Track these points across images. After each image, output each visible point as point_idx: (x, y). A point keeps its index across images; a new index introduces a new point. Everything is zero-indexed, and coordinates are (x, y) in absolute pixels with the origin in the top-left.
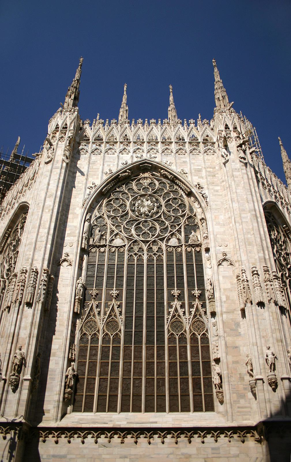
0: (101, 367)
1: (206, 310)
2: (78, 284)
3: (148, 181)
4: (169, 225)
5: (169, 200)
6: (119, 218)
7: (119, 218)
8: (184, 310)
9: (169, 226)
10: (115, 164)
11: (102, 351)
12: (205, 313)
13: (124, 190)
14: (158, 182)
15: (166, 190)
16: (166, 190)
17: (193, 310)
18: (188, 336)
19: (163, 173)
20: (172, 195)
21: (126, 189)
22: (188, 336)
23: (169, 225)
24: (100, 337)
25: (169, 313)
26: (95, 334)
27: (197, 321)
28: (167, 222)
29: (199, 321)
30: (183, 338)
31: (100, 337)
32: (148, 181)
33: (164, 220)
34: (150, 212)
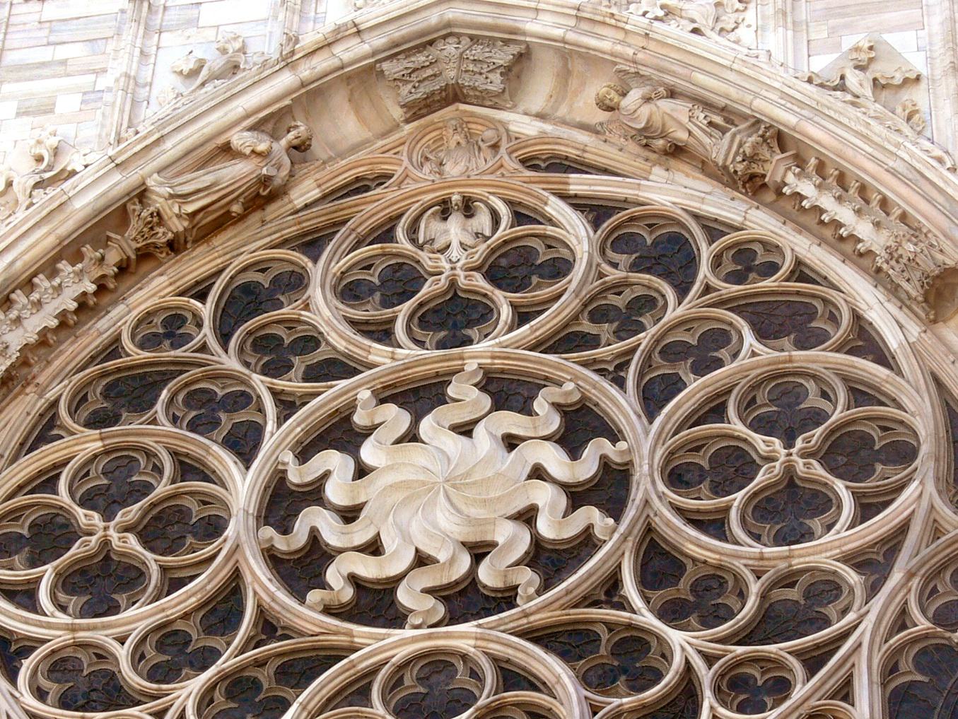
3: (482, 221)
4: (698, 663)
5: (714, 409)
6: (123, 653)
7: (123, 653)
9: (706, 676)
10: (104, 82)
13: (203, 348)
14: (596, 224)
15: (682, 291)
16: (682, 291)
19: (645, 111)
20: (749, 339)
21: (224, 339)
23: (698, 663)
28: (676, 638)
32: (482, 221)
33: (648, 619)
34: (479, 551)
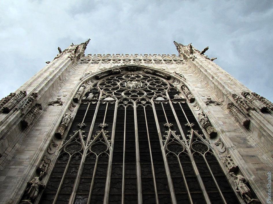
0: (80, 183)
1: (204, 135)
2: (66, 115)
8: (180, 136)
11: (84, 169)
12: (204, 138)
17: (191, 137)
18: (191, 155)
22: (191, 155)
24: (84, 156)
25: (164, 138)
26: (78, 154)
27: (197, 144)
29: (199, 144)
30: (185, 157)
31: (84, 156)
